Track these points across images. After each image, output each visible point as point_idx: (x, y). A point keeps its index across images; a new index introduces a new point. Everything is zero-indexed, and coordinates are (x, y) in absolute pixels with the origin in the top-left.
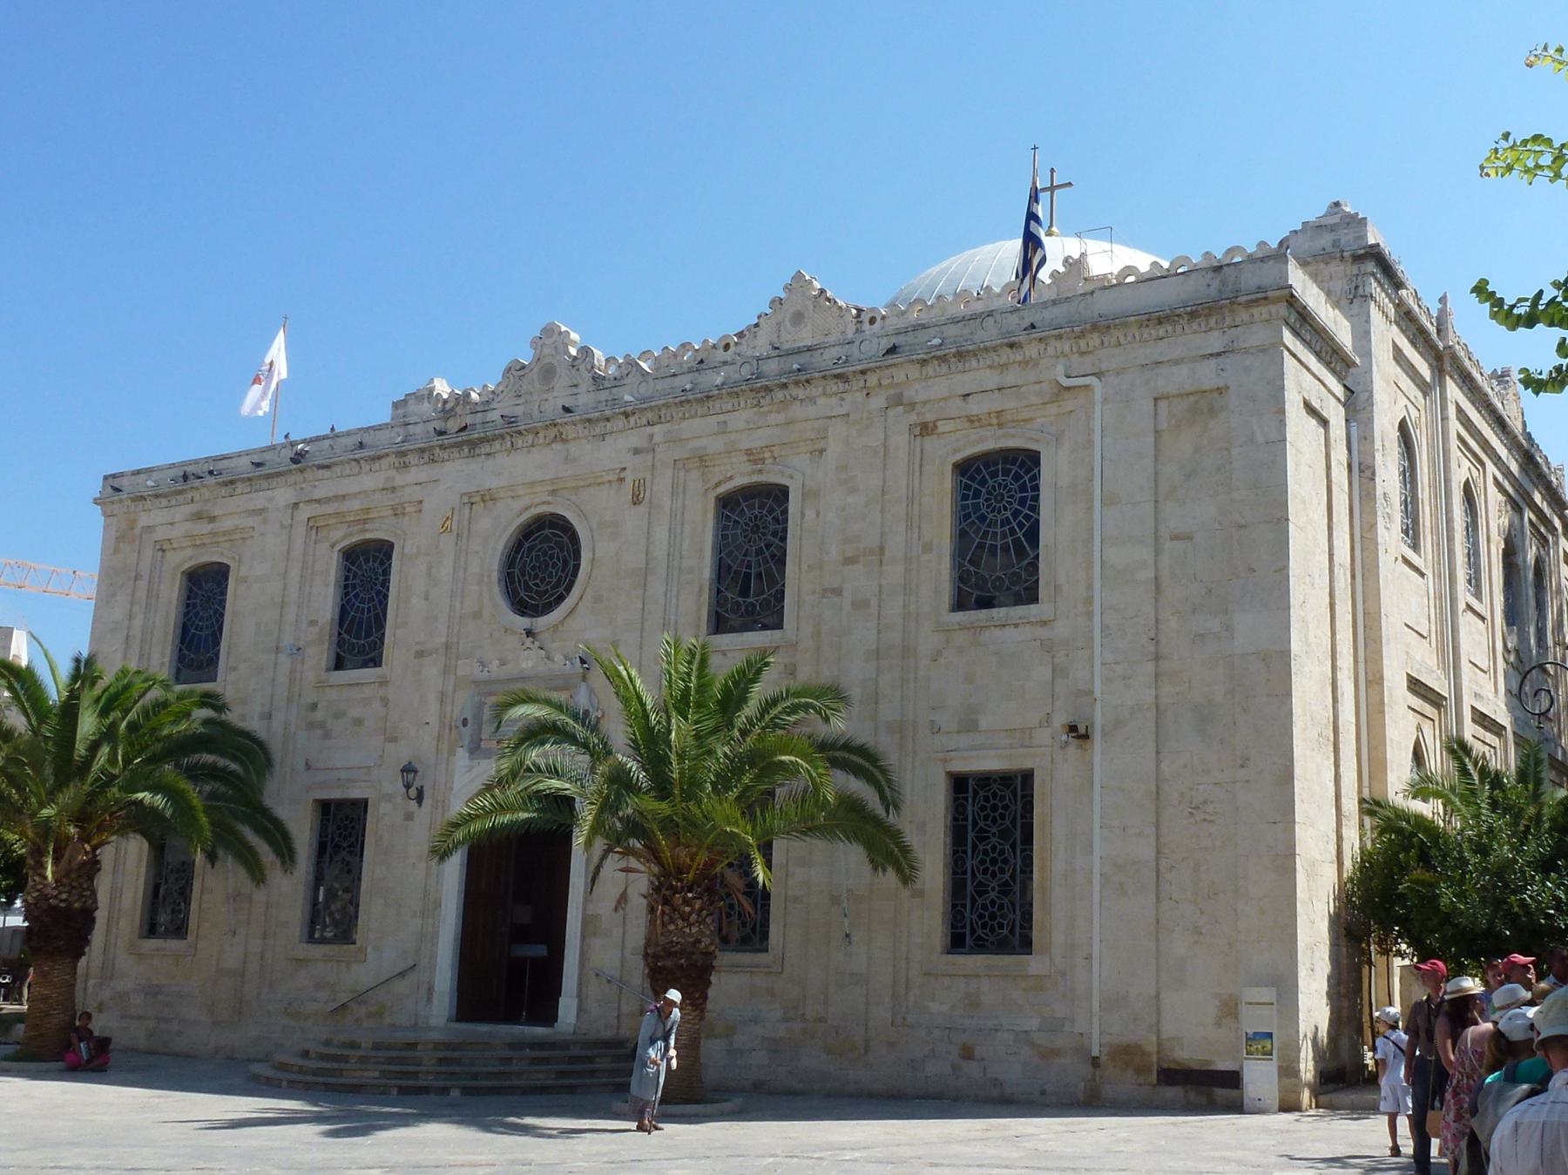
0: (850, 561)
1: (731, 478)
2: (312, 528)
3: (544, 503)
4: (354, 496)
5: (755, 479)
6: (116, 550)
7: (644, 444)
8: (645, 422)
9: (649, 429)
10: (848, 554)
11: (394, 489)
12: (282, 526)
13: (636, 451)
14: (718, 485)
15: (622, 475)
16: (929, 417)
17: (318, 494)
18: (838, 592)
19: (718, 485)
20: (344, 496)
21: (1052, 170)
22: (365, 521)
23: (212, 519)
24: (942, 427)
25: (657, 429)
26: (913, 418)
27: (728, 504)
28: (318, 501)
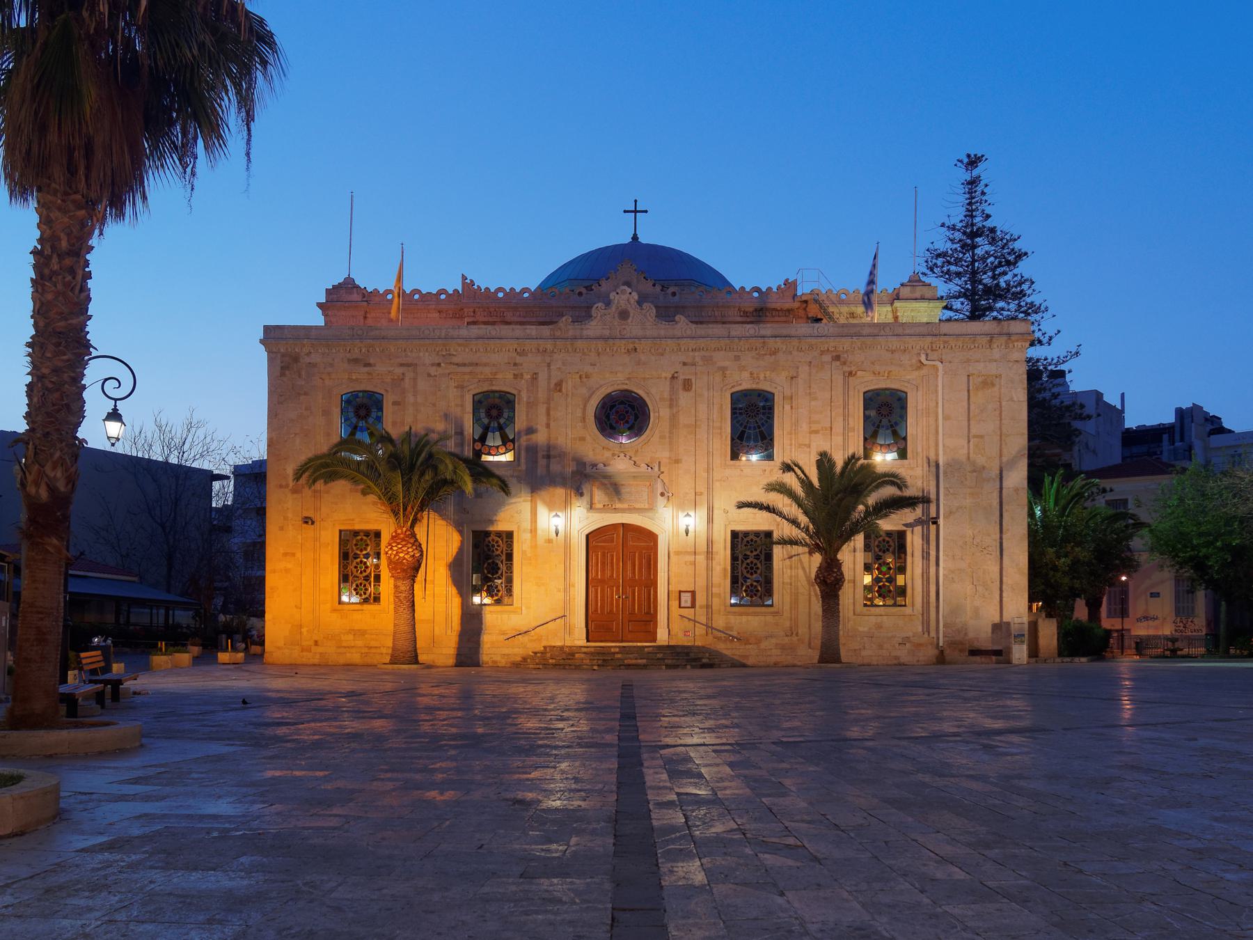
0: (816, 432)
1: (740, 385)
2: (451, 379)
3: (623, 384)
4: (486, 365)
5: (754, 386)
6: (283, 374)
7: (689, 360)
8: (690, 349)
9: (691, 354)
10: (812, 429)
11: (515, 364)
12: (429, 375)
13: (685, 364)
14: (733, 387)
15: (676, 375)
16: (853, 369)
17: (455, 360)
18: (809, 446)
19: (733, 387)
20: (477, 364)
21: (636, 201)
22: (491, 380)
23: (368, 365)
24: (859, 373)
25: (697, 354)
26: (846, 369)
27: (737, 398)
28: (457, 364)
